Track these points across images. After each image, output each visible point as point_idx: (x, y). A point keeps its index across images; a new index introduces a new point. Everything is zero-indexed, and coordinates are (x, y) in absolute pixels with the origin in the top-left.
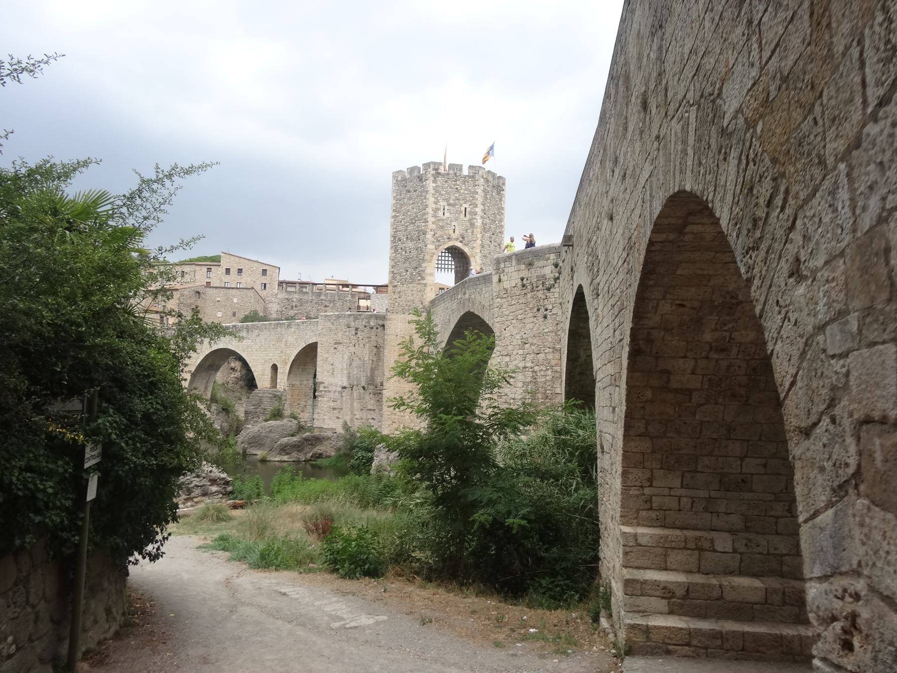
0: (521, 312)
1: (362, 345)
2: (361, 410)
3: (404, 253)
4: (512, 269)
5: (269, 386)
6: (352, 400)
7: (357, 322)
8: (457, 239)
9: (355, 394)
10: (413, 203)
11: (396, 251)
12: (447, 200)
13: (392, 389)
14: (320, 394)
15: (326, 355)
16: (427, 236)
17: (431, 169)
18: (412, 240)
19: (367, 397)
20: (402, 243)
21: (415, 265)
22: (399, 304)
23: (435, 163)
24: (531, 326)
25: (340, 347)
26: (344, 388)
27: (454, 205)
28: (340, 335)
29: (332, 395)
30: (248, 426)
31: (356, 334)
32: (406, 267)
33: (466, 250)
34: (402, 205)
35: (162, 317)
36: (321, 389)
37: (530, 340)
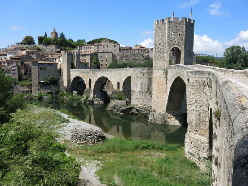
0: (195, 91)
2: (146, 99)
4: (192, 76)
5: (117, 89)
6: (143, 96)
8: (176, 45)
10: (161, 32)
12: (172, 31)
15: (134, 81)
16: (166, 44)
17: (167, 20)
18: (161, 45)
19: (147, 95)
20: (158, 46)
21: (162, 54)
23: (169, 18)
24: (199, 97)
25: (138, 79)
26: (140, 92)
27: (175, 33)
28: (138, 75)
29: (136, 94)
30: (112, 102)
33: (180, 48)
34: (157, 33)
35: (85, 64)
36: (133, 92)
37: (198, 101)
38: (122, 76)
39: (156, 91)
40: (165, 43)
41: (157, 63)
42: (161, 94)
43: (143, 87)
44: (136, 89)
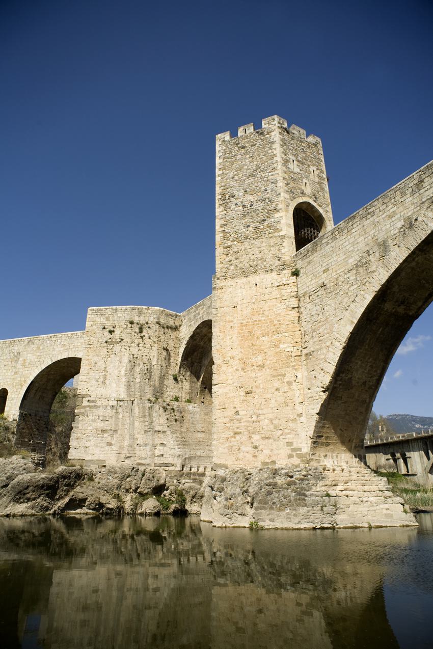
1: (148, 346)
8: (311, 197)
9: (136, 410)
14: (82, 410)
15: (96, 359)
25: (117, 348)
27: (303, 164)
29: (101, 412)
31: (141, 332)
33: (321, 211)
38: (24, 364)
39: (236, 363)
41: (237, 252)
42: (267, 371)
43: (138, 380)
44: (102, 391)
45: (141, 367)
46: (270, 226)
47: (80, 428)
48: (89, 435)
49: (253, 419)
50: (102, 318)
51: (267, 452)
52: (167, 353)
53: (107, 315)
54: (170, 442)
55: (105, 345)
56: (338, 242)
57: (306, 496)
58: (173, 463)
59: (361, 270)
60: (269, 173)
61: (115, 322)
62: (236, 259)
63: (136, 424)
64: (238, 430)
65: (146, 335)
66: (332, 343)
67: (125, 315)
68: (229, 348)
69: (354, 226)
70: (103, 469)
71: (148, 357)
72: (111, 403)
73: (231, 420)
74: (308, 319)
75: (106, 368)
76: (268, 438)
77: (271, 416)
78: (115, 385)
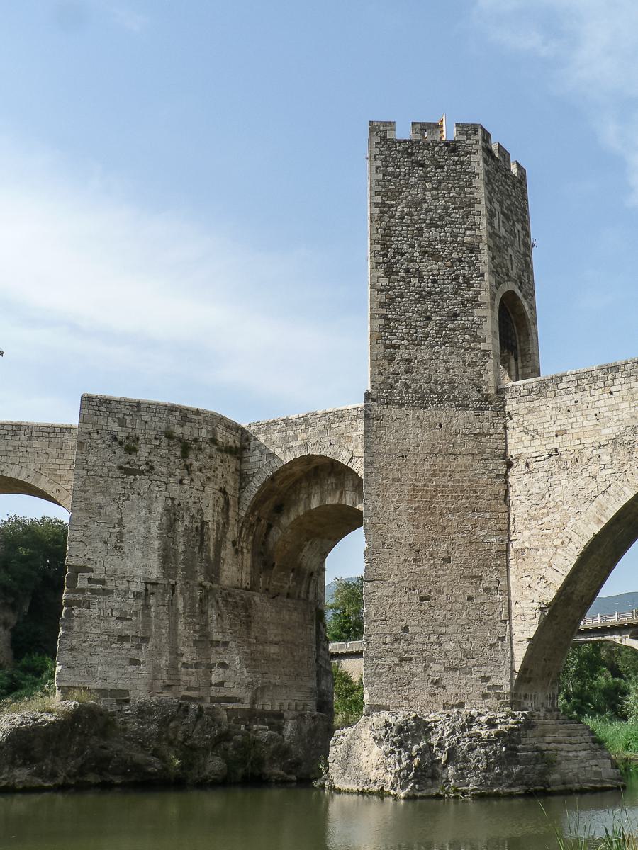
1: (198, 485)
3: (415, 280)
7: (187, 430)
11: (390, 273)
13: (397, 580)
14: (78, 597)
15: (99, 499)
22: (407, 386)
25: (142, 483)
29: (115, 601)
32: (426, 310)
40: (474, 250)
41: (409, 361)
42: (454, 570)
43: (181, 548)
44: (113, 562)
45: (186, 523)
46: (467, 330)
47: (76, 629)
48: (96, 643)
49: (431, 640)
50: (110, 419)
51: (452, 690)
52: (225, 498)
53: (120, 415)
54: (234, 661)
55: (118, 473)
56: (584, 397)
57: (518, 750)
58: (240, 696)
59: (621, 451)
60: (466, 229)
61: (138, 431)
62: (407, 372)
63: (180, 627)
64: (406, 655)
65: (194, 462)
66: (563, 543)
67: (157, 420)
68: (394, 525)
69: (616, 382)
70: (126, 707)
71: (198, 506)
72: (133, 587)
73: (396, 640)
74: (523, 498)
75: (121, 519)
76: (454, 669)
77: (459, 637)
78: (140, 554)
